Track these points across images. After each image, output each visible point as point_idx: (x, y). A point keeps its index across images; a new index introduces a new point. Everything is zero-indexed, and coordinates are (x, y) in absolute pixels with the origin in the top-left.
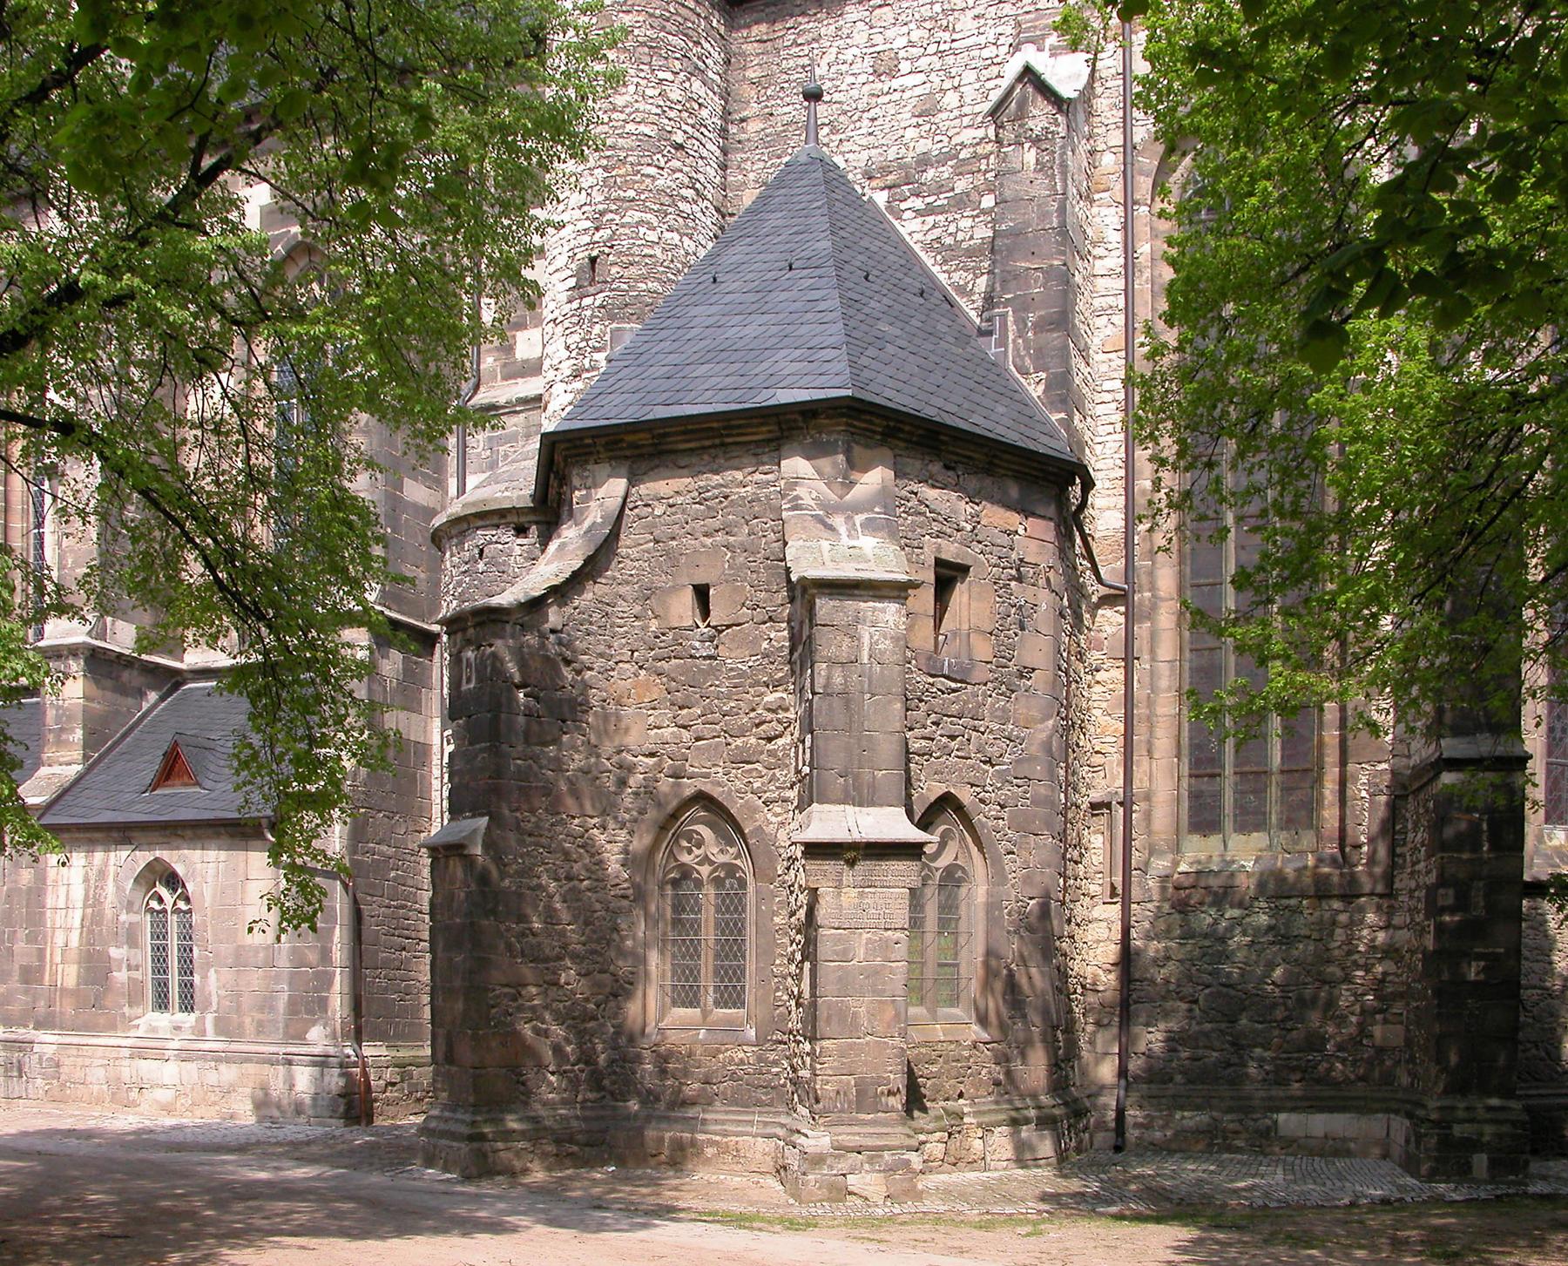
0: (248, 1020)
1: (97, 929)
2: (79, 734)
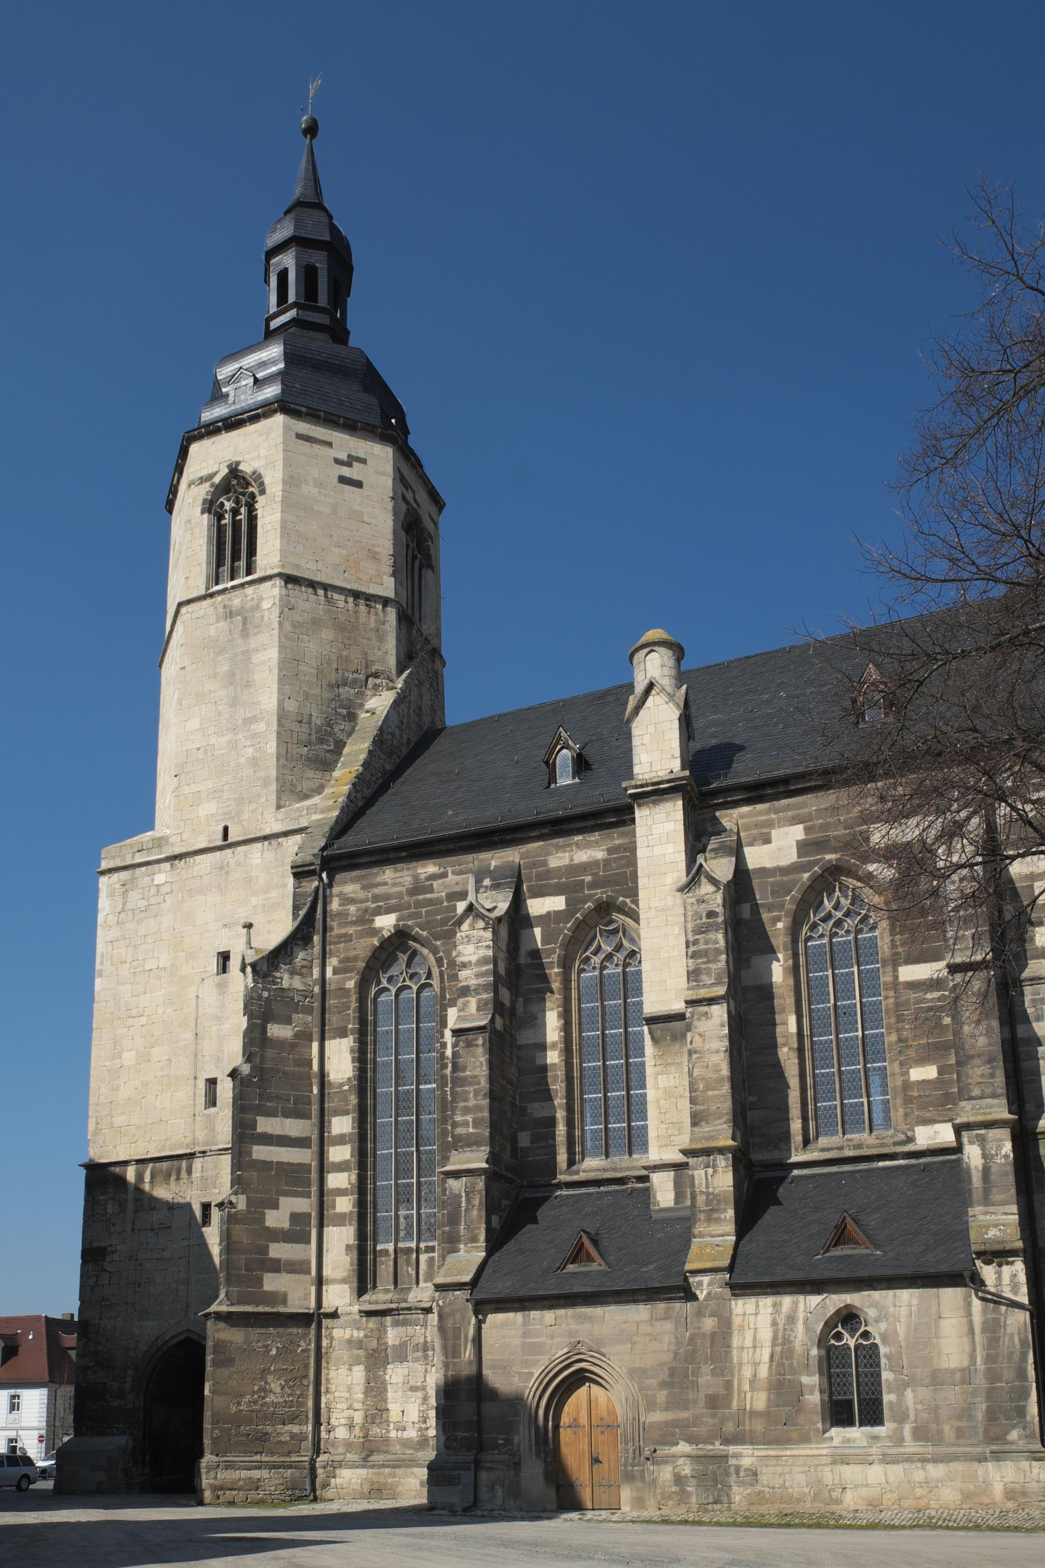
0: (946, 1428)
1: (786, 1362)
2: (730, 1213)
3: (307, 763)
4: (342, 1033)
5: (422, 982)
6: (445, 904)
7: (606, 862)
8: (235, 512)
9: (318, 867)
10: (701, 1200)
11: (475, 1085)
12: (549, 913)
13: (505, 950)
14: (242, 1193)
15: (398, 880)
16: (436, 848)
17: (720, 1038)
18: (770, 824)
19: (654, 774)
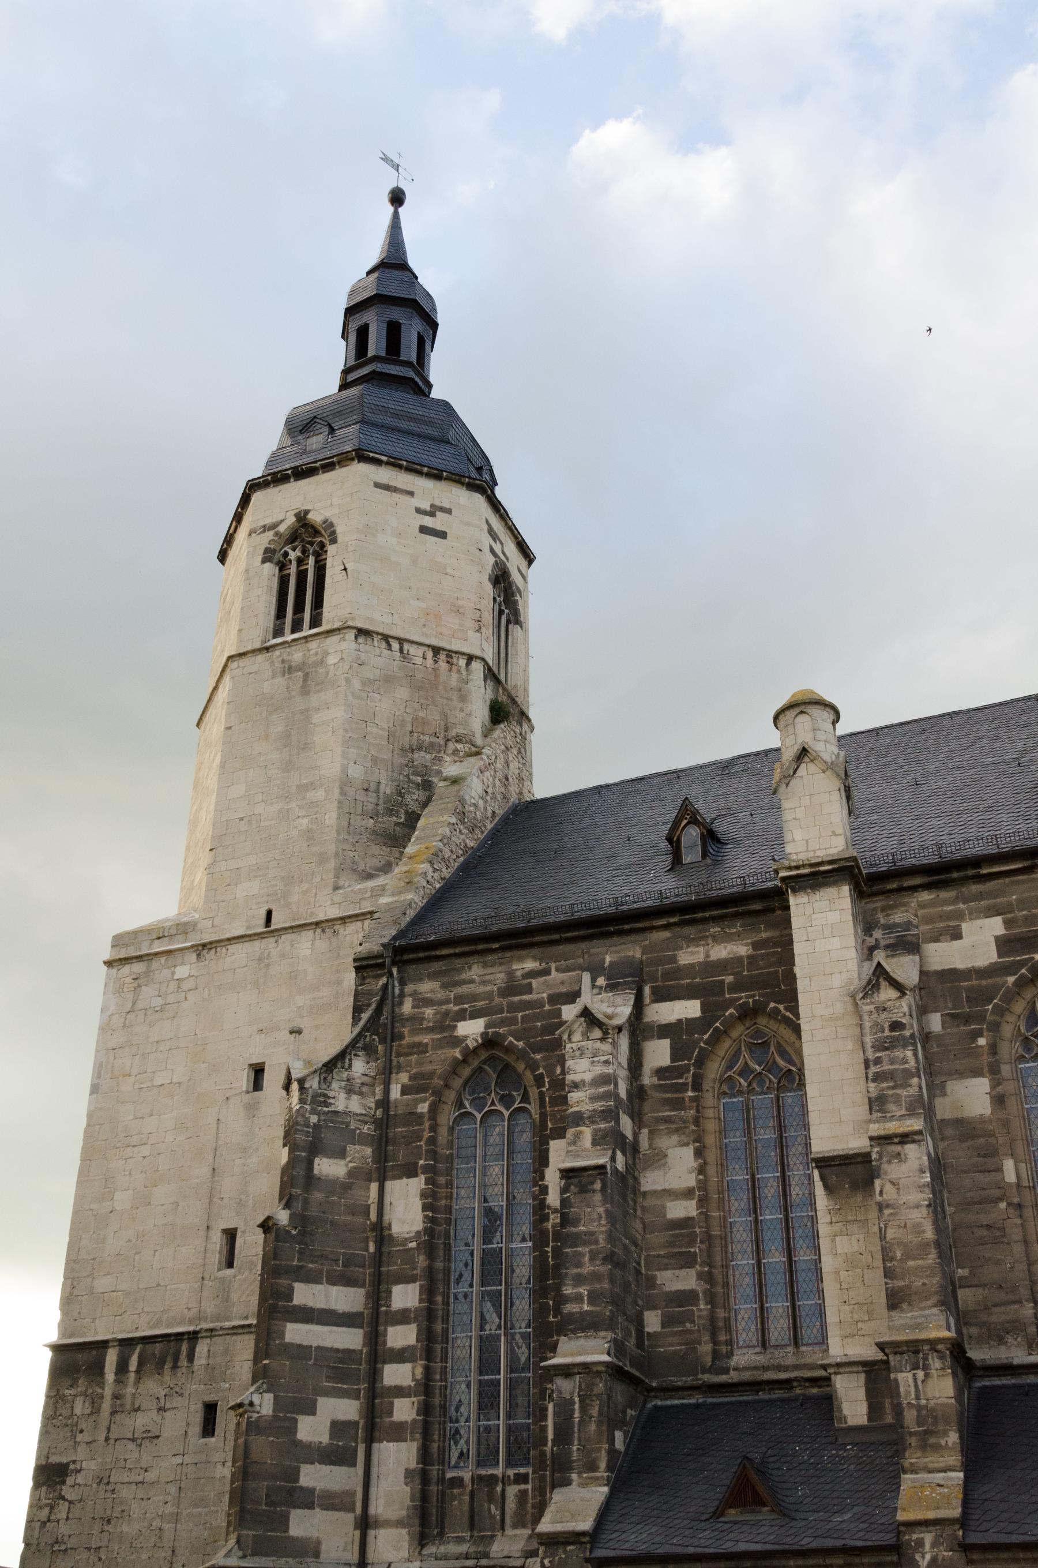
2: (953, 1437)
3: (373, 837)
4: (411, 1172)
5: (516, 1105)
6: (547, 1007)
8: (300, 561)
9: (388, 961)
10: (910, 1417)
11: (591, 1244)
12: (680, 1021)
13: (626, 1067)
14: (267, 1391)
15: (488, 978)
16: (537, 939)
17: (921, 1188)
18: (960, 916)
19: (812, 854)
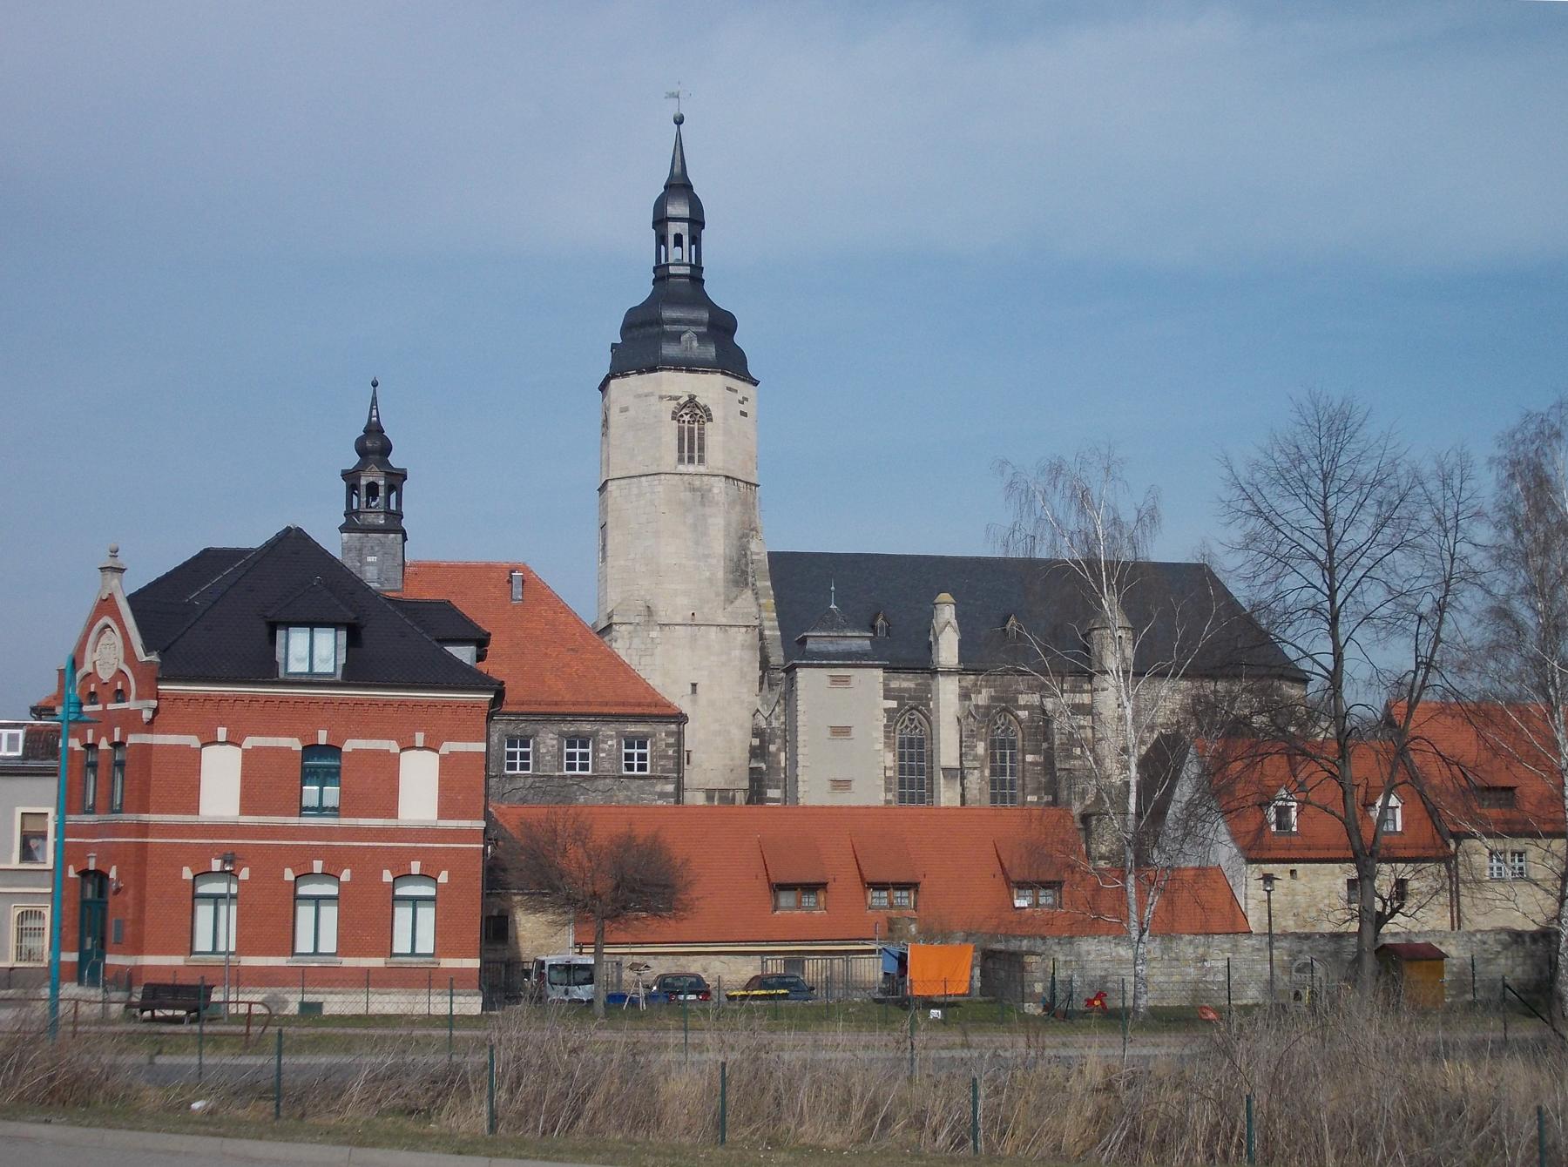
7: (915, 690)
